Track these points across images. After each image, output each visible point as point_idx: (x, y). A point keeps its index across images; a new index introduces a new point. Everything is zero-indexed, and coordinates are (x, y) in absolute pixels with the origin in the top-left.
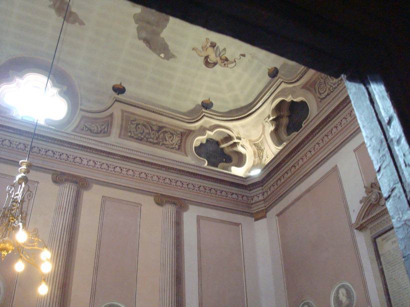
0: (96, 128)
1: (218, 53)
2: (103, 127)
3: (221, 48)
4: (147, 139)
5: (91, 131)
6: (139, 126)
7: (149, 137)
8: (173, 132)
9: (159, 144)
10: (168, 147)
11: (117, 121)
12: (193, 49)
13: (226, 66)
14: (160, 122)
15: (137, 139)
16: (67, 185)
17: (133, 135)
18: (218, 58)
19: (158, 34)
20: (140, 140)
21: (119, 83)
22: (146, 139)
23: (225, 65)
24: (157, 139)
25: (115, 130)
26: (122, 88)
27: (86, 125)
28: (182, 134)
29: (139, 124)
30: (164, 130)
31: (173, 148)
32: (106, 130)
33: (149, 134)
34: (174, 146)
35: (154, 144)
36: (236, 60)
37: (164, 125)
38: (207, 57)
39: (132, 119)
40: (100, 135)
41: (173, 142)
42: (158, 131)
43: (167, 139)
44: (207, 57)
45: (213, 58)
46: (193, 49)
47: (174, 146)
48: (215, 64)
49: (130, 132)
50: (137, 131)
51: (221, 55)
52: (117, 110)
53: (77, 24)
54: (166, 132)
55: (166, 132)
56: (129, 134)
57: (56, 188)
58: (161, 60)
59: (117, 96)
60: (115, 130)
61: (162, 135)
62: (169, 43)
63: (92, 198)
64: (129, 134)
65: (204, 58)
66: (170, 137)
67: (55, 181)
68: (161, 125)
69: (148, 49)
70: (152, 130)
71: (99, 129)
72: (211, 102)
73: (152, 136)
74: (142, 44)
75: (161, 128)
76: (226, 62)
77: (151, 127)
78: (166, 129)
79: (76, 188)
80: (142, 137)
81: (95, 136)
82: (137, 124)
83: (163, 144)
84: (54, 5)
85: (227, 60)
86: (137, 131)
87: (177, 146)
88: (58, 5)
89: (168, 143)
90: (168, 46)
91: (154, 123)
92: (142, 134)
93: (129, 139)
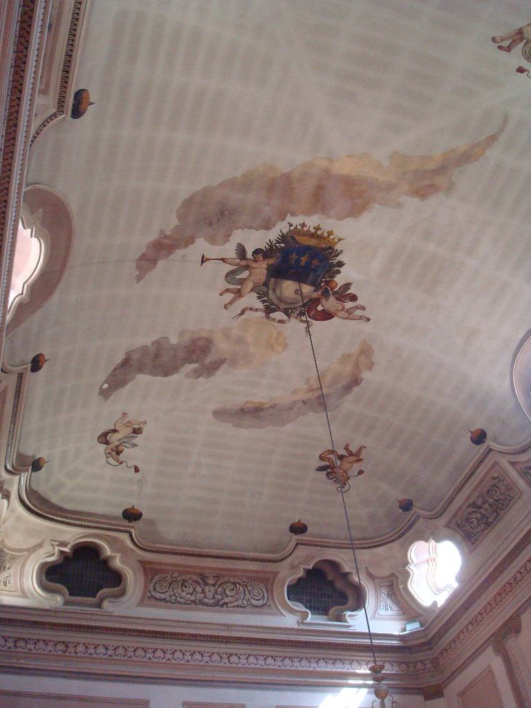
3: (135, 441)
13: (109, 455)
18: (117, 443)
44: (115, 431)
45: (114, 439)
48: (107, 443)
51: (123, 444)
65: (114, 428)
76: (114, 453)
85: (118, 453)
88: (165, 241)
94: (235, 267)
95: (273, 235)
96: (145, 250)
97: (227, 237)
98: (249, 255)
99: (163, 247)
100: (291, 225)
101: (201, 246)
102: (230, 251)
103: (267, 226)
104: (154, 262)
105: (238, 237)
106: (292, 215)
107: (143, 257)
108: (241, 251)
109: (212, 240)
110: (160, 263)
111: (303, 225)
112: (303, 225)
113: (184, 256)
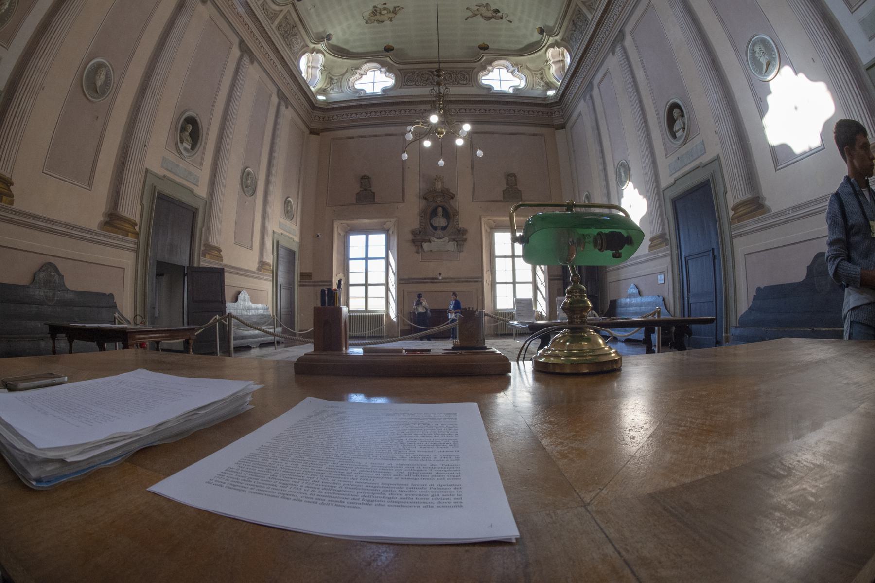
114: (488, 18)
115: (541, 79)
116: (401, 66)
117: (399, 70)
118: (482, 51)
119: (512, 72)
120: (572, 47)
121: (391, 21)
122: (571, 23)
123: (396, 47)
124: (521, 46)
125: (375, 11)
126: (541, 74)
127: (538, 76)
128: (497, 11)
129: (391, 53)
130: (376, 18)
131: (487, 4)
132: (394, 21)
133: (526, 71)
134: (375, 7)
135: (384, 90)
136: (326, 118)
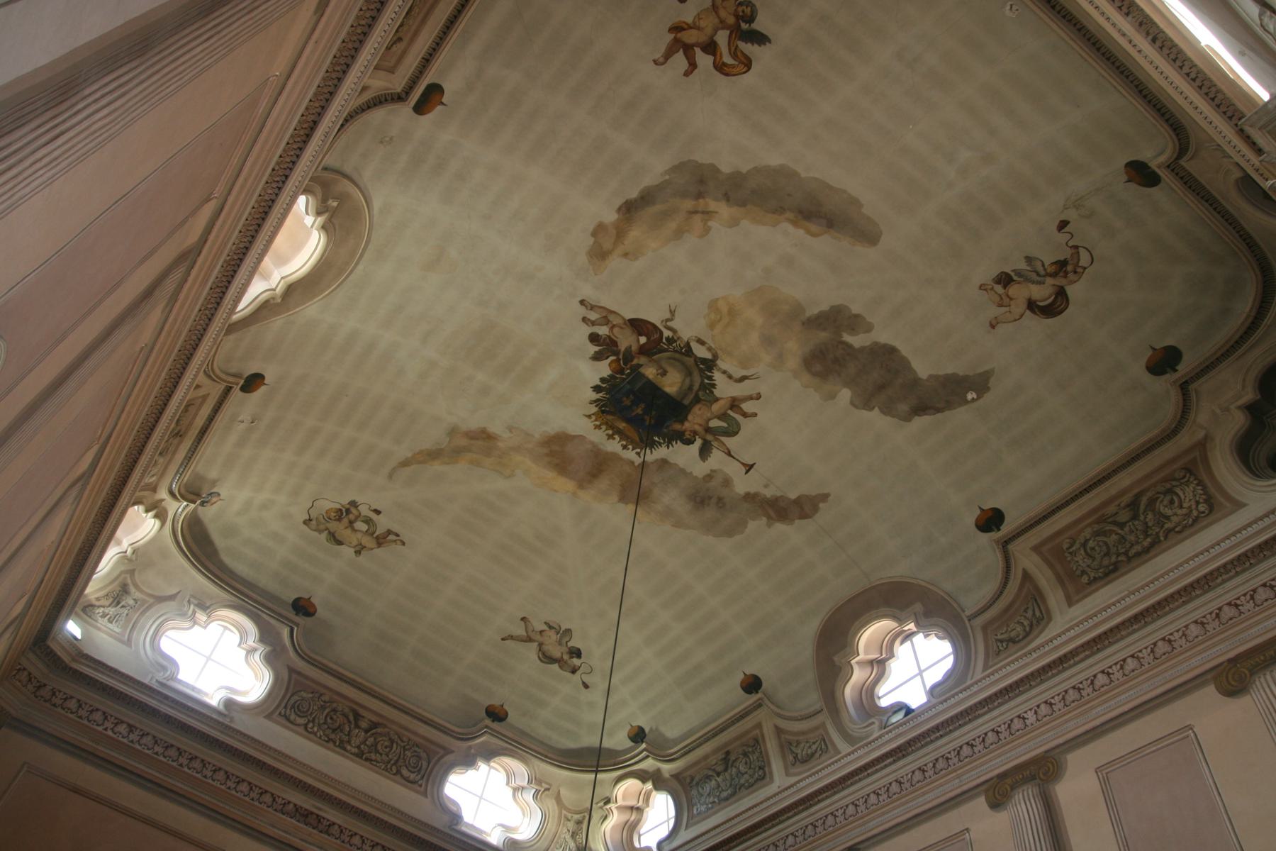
0: (1019, 629)
1: (1034, 276)
2: (1030, 614)
3: (1023, 265)
4: (1126, 553)
5: (1012, 641)
6: (1091, 544)
7: (1128, 545)
8: (1168, 486)
9: (1160, 541)
10: (1185, 527)
11: (1044, 578)
12: (993, 327)
13: (1079, 270)
14: (1123, 493)
15: (1106, 575)
16: (1018, 796)
17: (1092, 575)
18: (1049, 281)
19: (916, 381)
20: (1111, 572)
21: (978, 512)
22: (1122, 558)
23: (1075, 272)
24: (1147, 536)
25: (1054, 598)
26: (990, 514)
27: (1000, 637)
28: (1189, 470)
29: (1087, 541)
30: (1144, 500)
31: (1196, 520)
32: (1038, 614)
33: (1122, 539)
34: (1195, 513)
35: (1147, 550)
36: (1071, 244)
37: (1136, 491)
38: (1032, 305)
39: (1065, 546)
40: (1035, 632)
41: (1185, 505)
42: (1135, 517)
43: (1168, 512)
44: (1032, 305)
45: (1043, 293)
46: (993, 327)
47: (1195, 513)
48: (1061, 293)
49: (1083, 572)
50: (1094, 559)
51: (1042, 273)
52: (1026, 559)
53: (821, 505)
54: (1152, 502)
55: (1152, 502)
56: (1085, 579)
57: (1002, 818)
58: (981, 401)
59: (1000, 534)
60: (1054, 598)
61: (1150, 516)
62: (950, 369)
63: (1077, 788)
64: (1085, 579)
65: (1028, 312)
66: (1172, 502)
67: (996, 805)
68: (1126, 499)
69: (939, 415)
70: (1122, 525)
71: (1026, 623)
72: (1165, 348)
73: (1132, 538)
74: (920, 422)
75: (1133, 505)
76: (1069, 268)
77: (1115, 523)
78: (1149, 494)
79: (1036, 790)
80: (1113, 559)
81: (1029, 643)
82: (1084, 545)
83: (1170, 531)
84: (769, 517)
85: (1062, 264)
86: (1094, 559)
87: (1202, 507)
88: (772, 513)
89: (1175, 519)
90: (954, 375)
91: (1112, 509)
92: (1107, 554)
93: (1094, 587)
94: (723, 439)
95: (661, 452)
96: (797, 521)
97: (709, 477)
98: (698, 442)
99: (781, 510)
100: (638, 454)
101: (742, 484)
102: (717, 457)
103: (664, 463)
104: (798, 502)
105: (700, 469)
106: (633, 463)
107: (804, 516)
108: (705, 452)
109: (727, 482)
110: (793, 495)
111: (625, 447)
112: (625, 447)
113: (766, 486)
114: (547, 658)
115: (573, 835)
116: (301, 665)
117: (291, 670)
118: (488, 722)
119: (517, 790)
120: (690, 806)
121: (358, 553)
122: (721, 755)
123: (321, 612)
124: (572, 745)
125: (346, 513)
126: (579, 822)
127: (571, 825)
128: (577, 653)
129: (300, 620)
130: (333, 526)
131: (568, 631)
132: (362, 559)
133: (551, 804)
134: (353, 504)
135: (229, 704)
136: (45, 692)
